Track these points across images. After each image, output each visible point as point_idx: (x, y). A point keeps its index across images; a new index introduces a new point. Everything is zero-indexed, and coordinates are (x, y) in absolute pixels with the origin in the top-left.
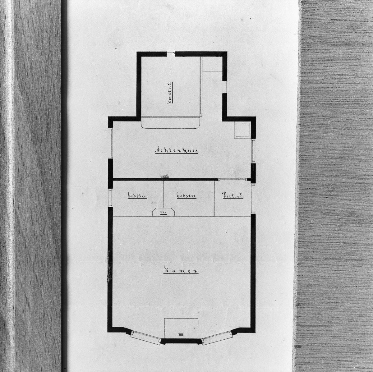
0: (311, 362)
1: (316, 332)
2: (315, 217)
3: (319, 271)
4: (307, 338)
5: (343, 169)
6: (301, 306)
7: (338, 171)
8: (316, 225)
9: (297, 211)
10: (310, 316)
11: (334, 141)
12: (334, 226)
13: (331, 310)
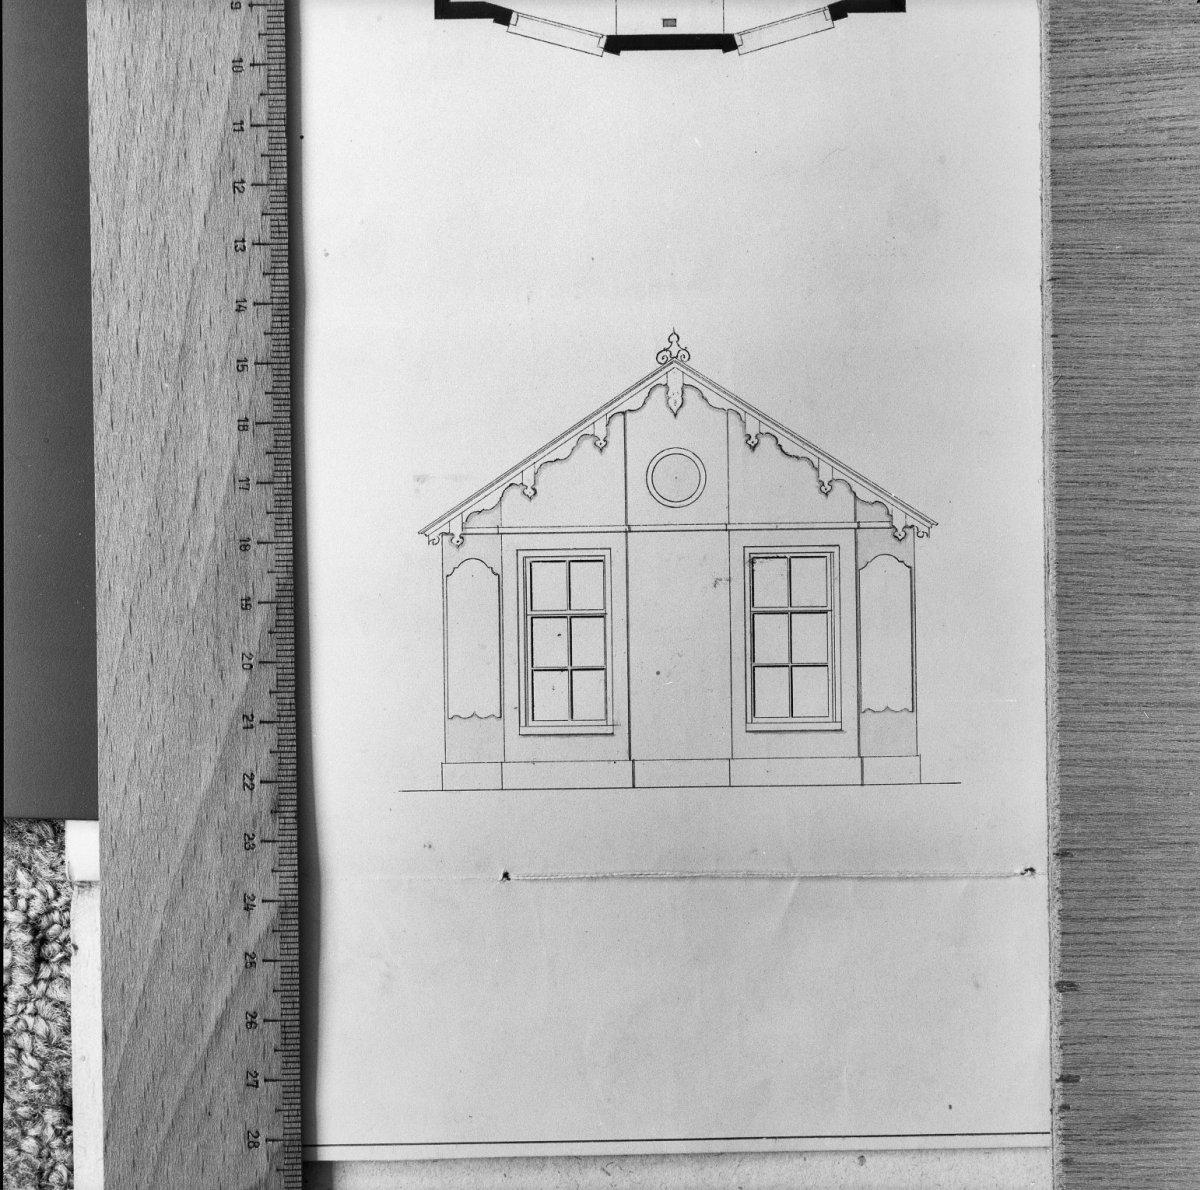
0: (1110, 1034)
1: (1122, 938)
2: (1108, 571)
3: (1127, 745)
4: (1094, 960)
5: (1194, 417)
6: (1072, 856)
7: (1180, 424)
8: (1114, 599)
9: (1053, 555)
10: (1102, 887)
11: (1164, 329)
12: (1172, 600)
13: (1170, 868)
